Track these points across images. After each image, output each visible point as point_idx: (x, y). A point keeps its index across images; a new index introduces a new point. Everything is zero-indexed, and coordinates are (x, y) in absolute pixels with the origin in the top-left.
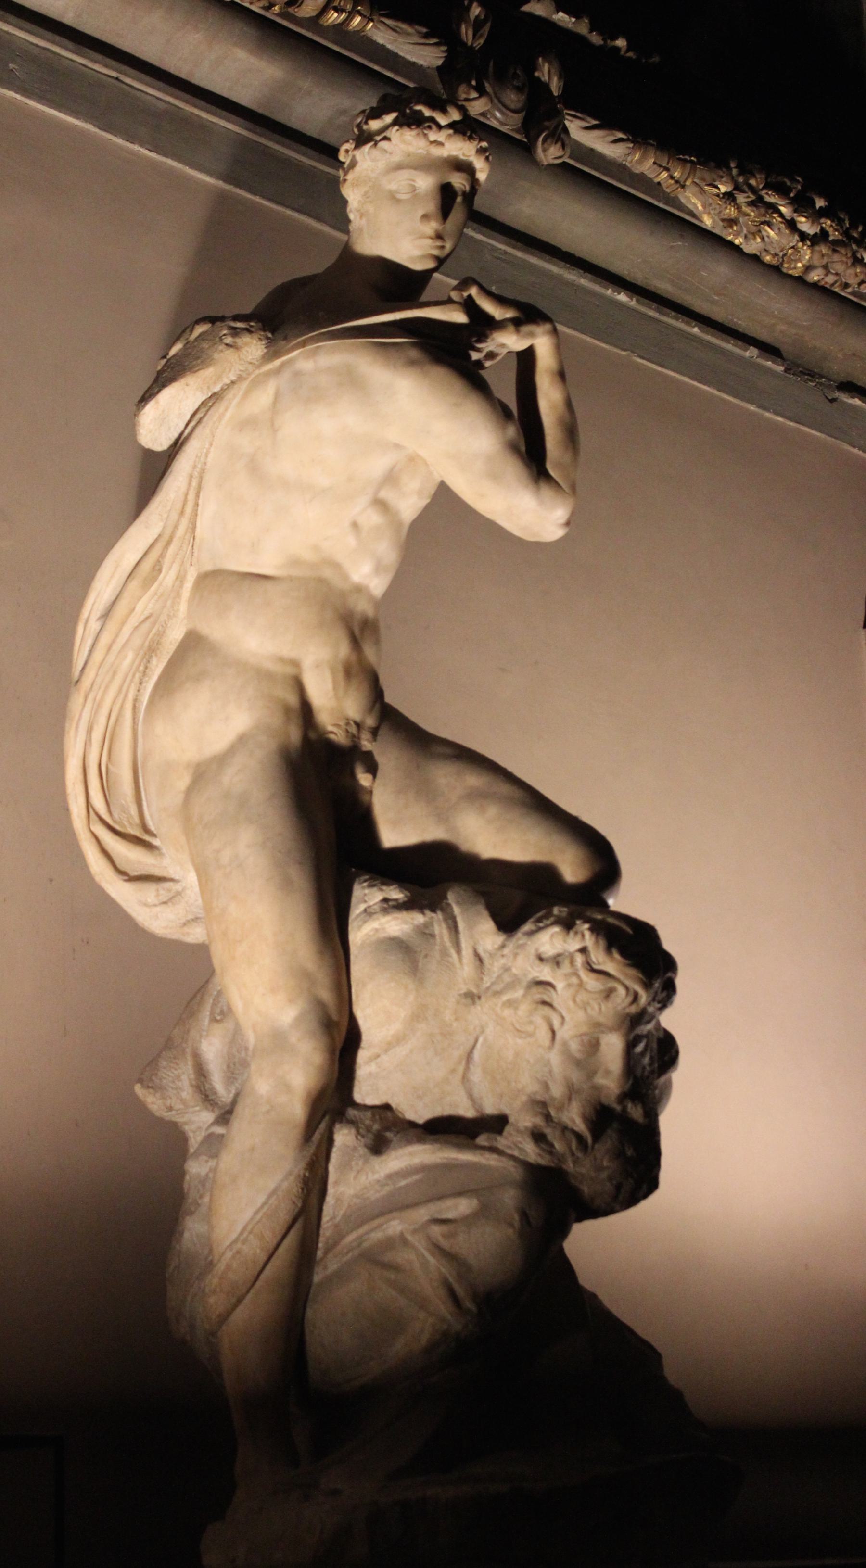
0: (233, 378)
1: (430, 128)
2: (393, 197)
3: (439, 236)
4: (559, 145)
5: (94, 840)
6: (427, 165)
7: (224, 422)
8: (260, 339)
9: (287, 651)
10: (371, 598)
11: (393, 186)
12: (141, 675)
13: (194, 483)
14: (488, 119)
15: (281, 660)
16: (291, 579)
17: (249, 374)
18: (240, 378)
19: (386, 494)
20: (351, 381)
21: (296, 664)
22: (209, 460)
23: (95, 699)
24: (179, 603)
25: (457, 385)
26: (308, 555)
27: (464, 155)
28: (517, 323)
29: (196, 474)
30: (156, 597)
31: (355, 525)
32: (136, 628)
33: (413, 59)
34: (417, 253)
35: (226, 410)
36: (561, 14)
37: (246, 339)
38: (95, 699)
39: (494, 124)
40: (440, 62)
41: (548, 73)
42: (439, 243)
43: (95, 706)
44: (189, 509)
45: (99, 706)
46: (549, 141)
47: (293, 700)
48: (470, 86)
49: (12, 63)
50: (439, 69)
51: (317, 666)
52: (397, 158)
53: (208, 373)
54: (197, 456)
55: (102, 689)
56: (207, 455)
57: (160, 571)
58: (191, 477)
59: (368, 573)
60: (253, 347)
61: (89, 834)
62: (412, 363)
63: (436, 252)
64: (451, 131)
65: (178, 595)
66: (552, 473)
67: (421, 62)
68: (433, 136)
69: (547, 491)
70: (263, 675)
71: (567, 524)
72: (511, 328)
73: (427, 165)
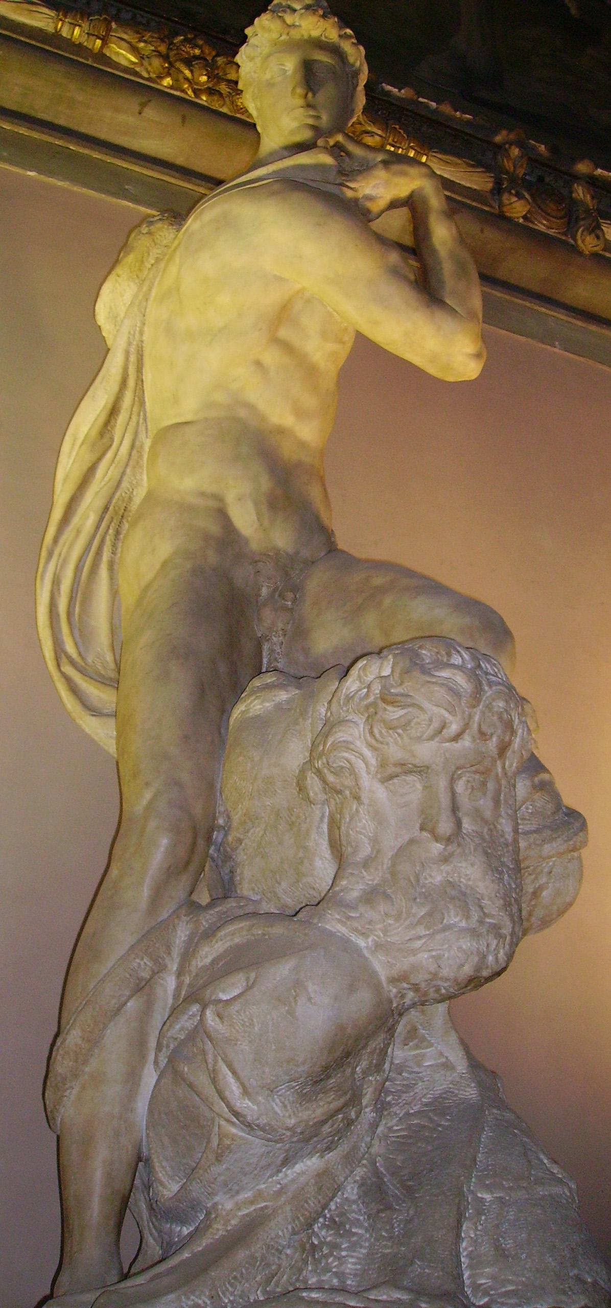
0: (153, 262)
1: (284, 11)
2: (270, 85)
3: (309, 106)
4: (593, 235)
5: (63, 680)
6: (292, 46)
7: (150, 302)
8: (172, 225)
9: (210, 488)
10: (302, 445)
11: (268, 76)
12: (113, 538)
13: (133, 358)
14: (533, 223)
15: (202, 494)
16: (206, 419)
17: (165, 255)
18: (158, 260)
19: (283, 333)
20: (226, 223)
21: (219, 498)
22: (144, 338)
23: (60, 555)
24: (141, 473)
25: (319, 208)
26: (220, 397)
27: (326, 37)
28: (386, 163)
29: (133, 349)
30: (114, 465)
31: (258, 364)
32: (97, 493)
33: (468, 185)
34: (294, 125)
35: (150, 289)
36: (599, 171)
37: (159, 225)
38: (60, 555)
39: (542, 228)
40: (490, 186)
41: (580, 192)
42: (312, 113)
43: (61, 560)
44: (131, 382)
45: (65, 561)
46: (585, 233)
47: (215, 529)
48: (511, 193)
49: (127, 184)
50: (492, 191)
51: (239, 500)
52: (266, 50)
53: (131, 258)
54: (129, 333)
55: (67, 544)
56: (141, 333)
57: (112, 440)
58: (127, 354)
59: (302, 426)
60: (165, 233)
61: (59, 674)
62: (273, 194)
63: (310, 121)
64: (303, 11)
65: (138, 464)
66: (448, 302)
67: (475, 187)
68: (289, 19)
69: (440, 315)
70: (185, 508)
71: (478, 356)
72: (380, 166)
73: (292, 46)
